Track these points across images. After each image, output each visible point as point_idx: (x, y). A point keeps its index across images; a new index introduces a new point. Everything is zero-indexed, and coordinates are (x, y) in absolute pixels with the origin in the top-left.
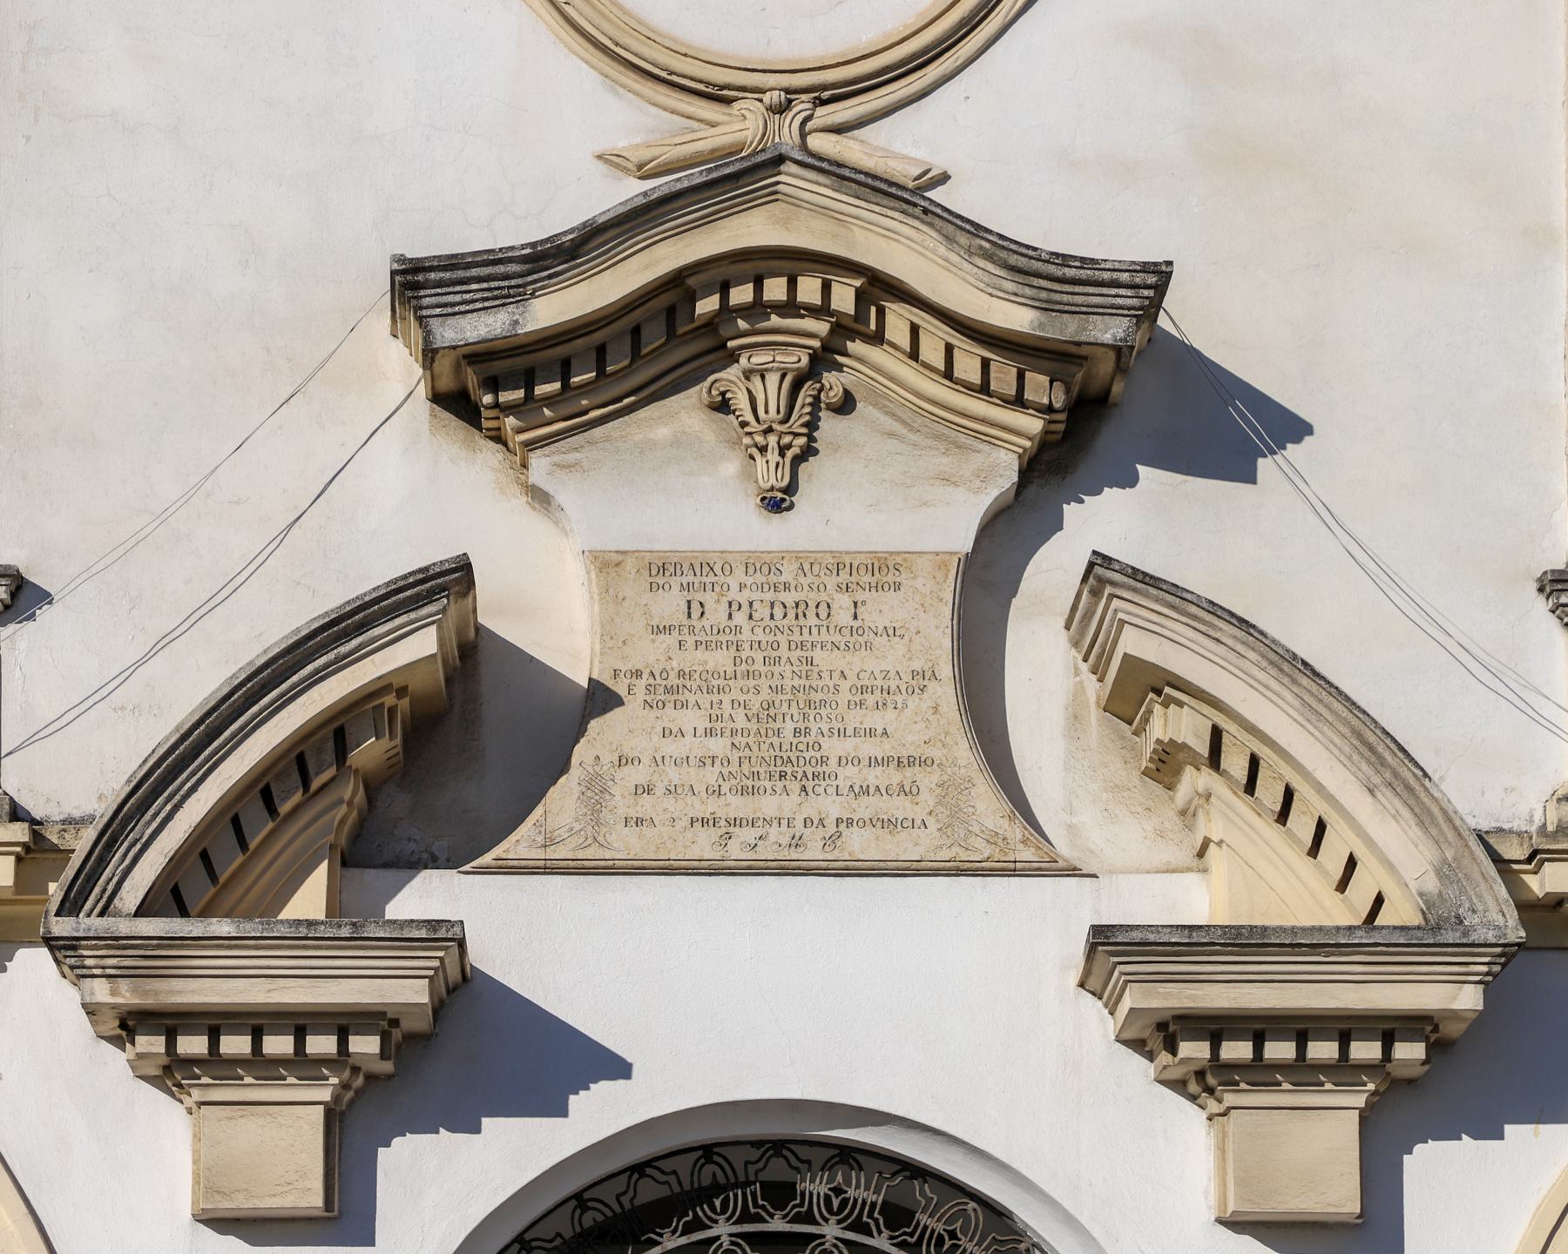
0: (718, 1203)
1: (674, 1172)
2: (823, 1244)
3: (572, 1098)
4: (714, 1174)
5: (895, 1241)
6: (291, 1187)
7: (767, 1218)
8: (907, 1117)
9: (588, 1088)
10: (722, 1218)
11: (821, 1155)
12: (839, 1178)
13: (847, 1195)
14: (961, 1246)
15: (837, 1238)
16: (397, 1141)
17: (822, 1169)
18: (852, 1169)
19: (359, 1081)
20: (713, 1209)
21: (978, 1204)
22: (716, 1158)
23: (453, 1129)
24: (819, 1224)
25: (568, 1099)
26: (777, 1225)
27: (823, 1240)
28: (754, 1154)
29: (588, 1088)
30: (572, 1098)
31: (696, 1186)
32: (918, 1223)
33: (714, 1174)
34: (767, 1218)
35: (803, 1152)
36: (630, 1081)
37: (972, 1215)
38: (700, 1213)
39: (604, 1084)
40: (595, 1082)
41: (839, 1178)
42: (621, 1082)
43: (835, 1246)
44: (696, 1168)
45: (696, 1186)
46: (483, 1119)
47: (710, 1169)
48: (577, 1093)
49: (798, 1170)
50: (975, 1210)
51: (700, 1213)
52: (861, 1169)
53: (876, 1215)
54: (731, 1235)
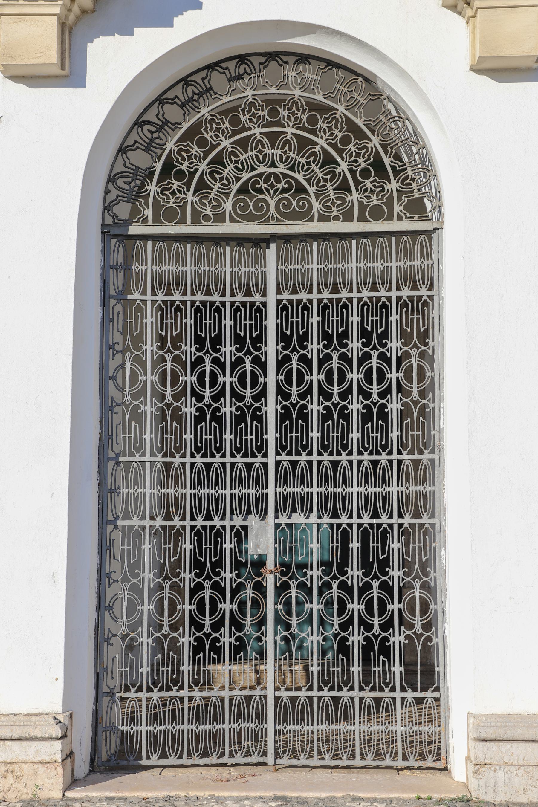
0: (246, 81)
1: (227, 68)
2: (294, 98)
3: (175, 19)
4: (245, 68)
5: (326, 96)
6: (42, 54)
7: (269, 88)
8: (328, 27)
9: (182, 14)
10: (249, 88)
11: (293, 59)
12: (301, 69)
13: (304, 77)
14: (354, 98)
15: (299, 96)
16: (96, 40)
17: (294, 64)
18: (306, 64)
19: (76, 9)
20: (244, 84)
21: (364, 80)
22: (246, 61)
23: (121, 34)
24: (292, 90)
25: (173, 19)
26: (273, 90)
27: (293, 97)
28: (263, 59)
29: (182, 14)
30: (175, 19)
31: (237, 74)
32: (336, 87)
33: (245, 68)
34: (269, 88)
35: (285, 58)
36: (201, 11)
37: (360, 83)
38: (239, 86)
39: (190, 12)
40: (186, 11)
41: (301, 69)
42: (198, 11)
43: (299, 99)
44: (237, 66)
45: (237, 74)
46: (135, 29)
47: (243, 67)
48: (178, 17)
49: (281, 65)
50: (361, 82)
51: (239, 86)
52: (310, 64)
53: (317, 85)
54: (252, 95)
